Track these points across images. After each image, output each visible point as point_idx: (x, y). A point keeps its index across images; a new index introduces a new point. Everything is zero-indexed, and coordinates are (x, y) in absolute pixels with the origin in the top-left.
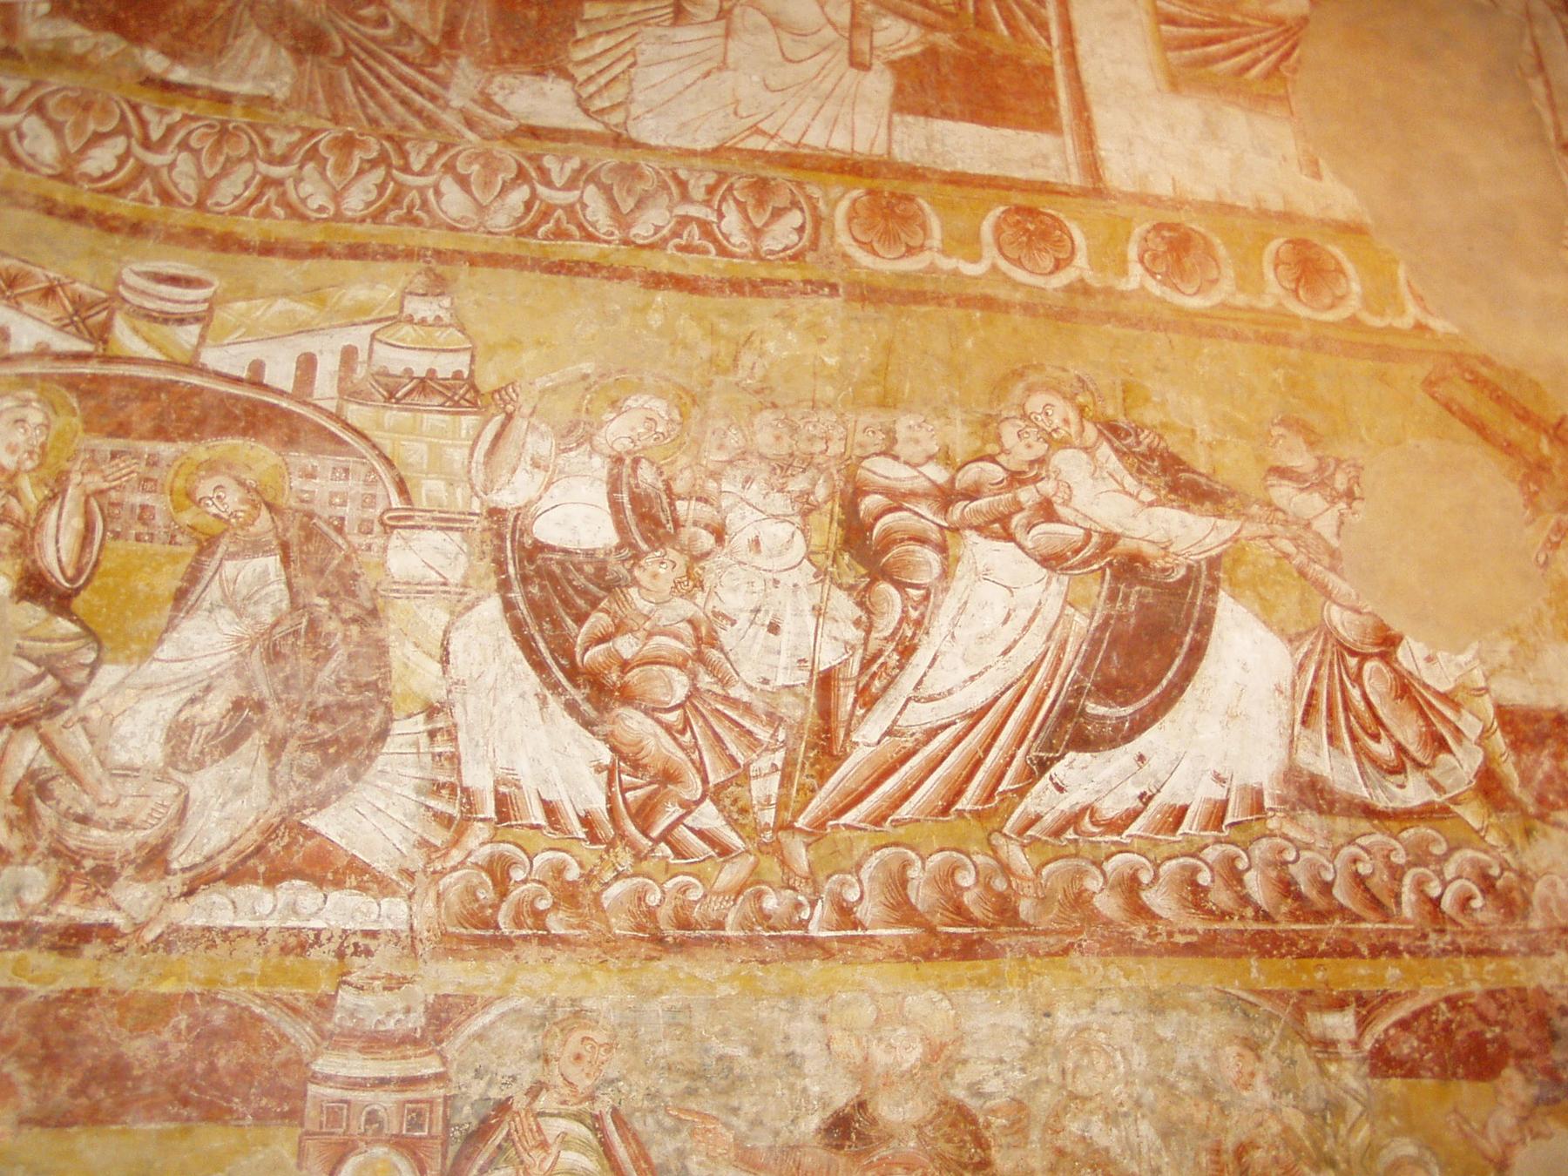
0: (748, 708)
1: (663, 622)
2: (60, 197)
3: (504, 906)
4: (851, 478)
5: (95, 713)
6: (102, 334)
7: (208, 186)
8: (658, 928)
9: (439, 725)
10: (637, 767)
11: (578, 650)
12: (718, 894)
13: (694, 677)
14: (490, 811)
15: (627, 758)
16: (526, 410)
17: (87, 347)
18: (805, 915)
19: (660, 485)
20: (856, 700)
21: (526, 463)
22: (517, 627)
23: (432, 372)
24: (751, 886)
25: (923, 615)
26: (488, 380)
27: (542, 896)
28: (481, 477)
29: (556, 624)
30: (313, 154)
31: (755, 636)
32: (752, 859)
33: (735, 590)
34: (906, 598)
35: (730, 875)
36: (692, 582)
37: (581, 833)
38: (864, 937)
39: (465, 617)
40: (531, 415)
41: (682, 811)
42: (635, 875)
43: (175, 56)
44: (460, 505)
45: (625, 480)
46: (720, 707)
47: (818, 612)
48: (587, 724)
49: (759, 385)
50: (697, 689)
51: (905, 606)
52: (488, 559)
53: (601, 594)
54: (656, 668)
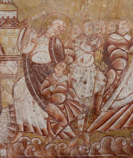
0: (78, 103)
1: (60, 82)
3: (26, 151)
4: (106, 40)
8: (57, 154)
9: (12, 110)
10: (54, 118)
11: (41, 90)
12: (70, 147)
13: (66, 96)
14: (22, 129)
15: (51, 116)
16: (30, 27)
18: (88, 152)
19: (61, 45)
20: (102, 101)
21: (30, 42)
22: (28, 85)
23: (8, 17)
24: (76, 146)
25: (120, 78)
26: (21, 19)
27: (33, 148)
28: (20, 46)
29: (37, 84)
31: (81, 85)
32: (77, 139)
33: (77, 73)
34: (117, 73)
35: (72, 143)
36: (67, 71)
37: (41, 134)
38: (100, 156)
39: (17, 83)
40: (31, 27)
41: (62, 128)
42: (52, 143)
44: (16, 54)
45: (53, 44)
46: (72, 103)
47: (96, 78)
48: (43, 108)
49: (85, 14)
50: (67, 99)
51: (116, 75)
52: (22, 67)
53: (47, 75)
54: (58, 94)
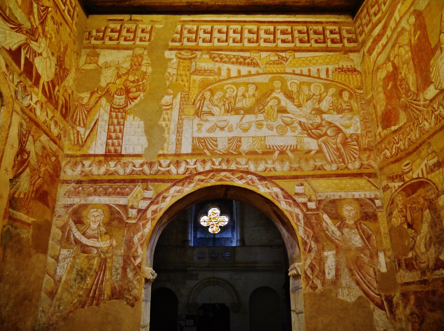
2: (393, 160)
5: (418, 245)
6: (403, 180)
7: (404, 145)
17: (403, 183)
30: (412, 130)
43: (395, 125)
